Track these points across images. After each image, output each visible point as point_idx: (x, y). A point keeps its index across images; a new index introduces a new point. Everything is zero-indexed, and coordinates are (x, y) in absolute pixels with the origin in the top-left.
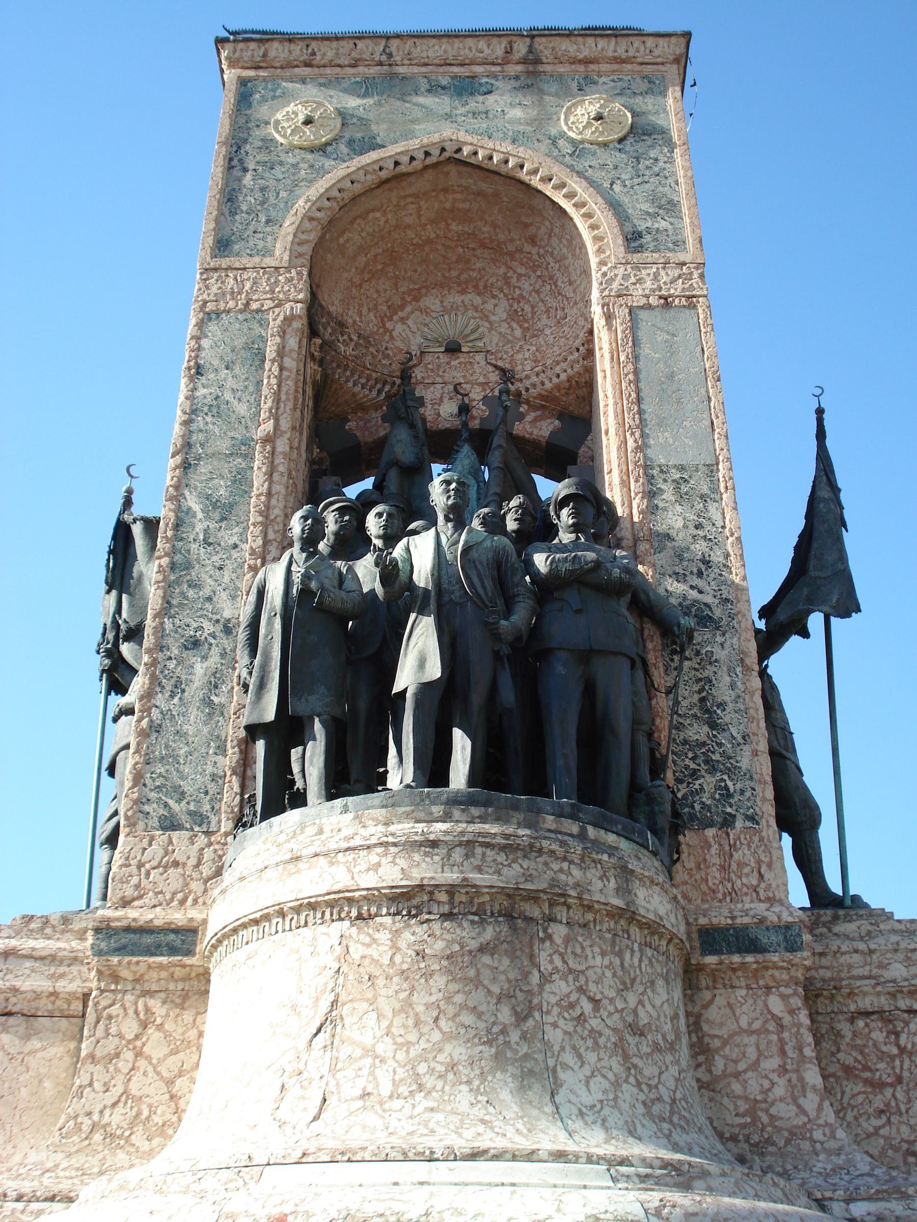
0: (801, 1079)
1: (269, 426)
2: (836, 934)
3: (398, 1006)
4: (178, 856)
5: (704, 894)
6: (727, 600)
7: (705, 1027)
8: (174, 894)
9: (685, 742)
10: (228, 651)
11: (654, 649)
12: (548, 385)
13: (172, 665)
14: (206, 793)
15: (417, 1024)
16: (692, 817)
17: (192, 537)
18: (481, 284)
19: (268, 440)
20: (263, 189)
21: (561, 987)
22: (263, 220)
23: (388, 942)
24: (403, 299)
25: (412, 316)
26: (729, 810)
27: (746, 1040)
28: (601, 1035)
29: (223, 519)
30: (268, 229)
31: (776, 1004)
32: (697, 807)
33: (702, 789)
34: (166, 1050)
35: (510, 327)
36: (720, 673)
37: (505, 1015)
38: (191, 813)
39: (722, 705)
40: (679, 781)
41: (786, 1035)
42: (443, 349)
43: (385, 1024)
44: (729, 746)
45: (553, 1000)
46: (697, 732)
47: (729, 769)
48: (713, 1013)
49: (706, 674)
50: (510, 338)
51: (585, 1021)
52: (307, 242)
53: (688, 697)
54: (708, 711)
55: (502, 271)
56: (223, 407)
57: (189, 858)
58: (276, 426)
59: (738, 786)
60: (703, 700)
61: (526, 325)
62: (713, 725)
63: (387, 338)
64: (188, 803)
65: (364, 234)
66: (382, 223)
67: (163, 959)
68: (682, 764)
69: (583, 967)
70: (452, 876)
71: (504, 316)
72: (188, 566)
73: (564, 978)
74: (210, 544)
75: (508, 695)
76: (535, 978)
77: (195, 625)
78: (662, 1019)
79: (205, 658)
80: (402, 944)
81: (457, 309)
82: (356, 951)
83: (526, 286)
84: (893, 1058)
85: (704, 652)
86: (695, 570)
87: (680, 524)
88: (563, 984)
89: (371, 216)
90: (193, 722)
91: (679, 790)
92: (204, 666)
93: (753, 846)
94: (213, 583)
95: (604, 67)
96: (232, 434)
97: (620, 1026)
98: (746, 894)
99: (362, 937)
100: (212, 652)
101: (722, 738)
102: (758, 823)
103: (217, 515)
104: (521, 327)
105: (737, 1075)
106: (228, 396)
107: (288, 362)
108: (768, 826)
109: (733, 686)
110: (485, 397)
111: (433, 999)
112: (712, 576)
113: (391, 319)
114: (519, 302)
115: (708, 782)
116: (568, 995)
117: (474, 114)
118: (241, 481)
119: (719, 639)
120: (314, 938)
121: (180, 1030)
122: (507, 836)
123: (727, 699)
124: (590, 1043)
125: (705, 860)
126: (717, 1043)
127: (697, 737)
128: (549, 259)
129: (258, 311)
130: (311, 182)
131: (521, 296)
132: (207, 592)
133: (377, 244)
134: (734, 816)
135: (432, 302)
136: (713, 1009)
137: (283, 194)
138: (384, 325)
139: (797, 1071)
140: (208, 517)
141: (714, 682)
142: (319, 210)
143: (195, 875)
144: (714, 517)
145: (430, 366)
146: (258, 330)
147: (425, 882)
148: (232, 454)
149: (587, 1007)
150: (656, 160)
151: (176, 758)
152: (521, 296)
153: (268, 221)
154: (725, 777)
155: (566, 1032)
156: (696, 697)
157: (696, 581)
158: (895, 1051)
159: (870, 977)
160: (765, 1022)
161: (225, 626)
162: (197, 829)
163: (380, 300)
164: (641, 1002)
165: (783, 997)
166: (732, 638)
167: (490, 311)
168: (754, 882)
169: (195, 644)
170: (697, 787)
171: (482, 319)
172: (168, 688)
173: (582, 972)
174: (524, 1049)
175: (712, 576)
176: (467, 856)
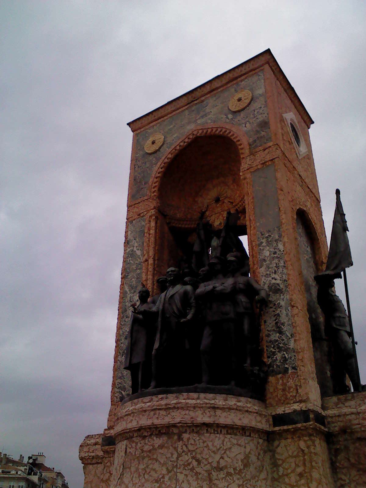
0: (311, 476)
1: (146, 256)
2: (346, 406)
9: (271, 341)
15: (140, 476)
16: (273, 371)
17: (127, 300)
19: (147, 260)
22: (143, 184)
23: (135, 447)
26: (286, 366)
28: (200, 474)
31: (302, 445)
32: (275, 367)
33: (277, 359)
36: (282, 311)
37: (164, 471)
39: (283, 324)
40: (269, 357)
41: (306, 457)
42: (214, 202)
44: (286, 340)
45: (182, 463)
46: (275, 336)
48: (279, 450)
49: (278, 312)
52: (156, 186)
58: (148, 255)
59: (289, 356)
60: (276, 323)
70: (149, 422)
71: (231, 182)
73: (186, 454)
76: (175, 456)
78: (235, 462)
80: (138, 447)
82: (128, 450)
85: (276, 304)
86: (274, 271)
87: (268, 254)
93: (294, 379)
95: (243, 78)
98: (292, 400)
101: (283, 337)
102: (297, 370)
103: (132, 291)
105: (287, 475)
106: (135, 249)
107: (152, 232)
108: (300, 370)
109: (287, 315)
115: (279, 356)
116: (187, 461)
122: (166, 405)
123: (285, 321)
124: (195, 478)
126: (280, 462)
127: (275, 338)
134: (288, 368)
136: (279, 448)
139: (310, 472)
140: (131, 293)
141: (280, 315)
142: (159, 173)
144: (280, 248)
147: (142, 425)
149: (195, 463)
150: (261, 107)
154: (285, 353)
155: (185, 475)
156: (275, 322)
159: (359, 424)
160: (298, 452)
164: (222, 458)
165: (305, 441)
166: (286, 295)
168: (294, 394)
170: (275, 358)
172: (121, 353)
173: (194, 451)
174: (168, 483)
176: (154, 414)
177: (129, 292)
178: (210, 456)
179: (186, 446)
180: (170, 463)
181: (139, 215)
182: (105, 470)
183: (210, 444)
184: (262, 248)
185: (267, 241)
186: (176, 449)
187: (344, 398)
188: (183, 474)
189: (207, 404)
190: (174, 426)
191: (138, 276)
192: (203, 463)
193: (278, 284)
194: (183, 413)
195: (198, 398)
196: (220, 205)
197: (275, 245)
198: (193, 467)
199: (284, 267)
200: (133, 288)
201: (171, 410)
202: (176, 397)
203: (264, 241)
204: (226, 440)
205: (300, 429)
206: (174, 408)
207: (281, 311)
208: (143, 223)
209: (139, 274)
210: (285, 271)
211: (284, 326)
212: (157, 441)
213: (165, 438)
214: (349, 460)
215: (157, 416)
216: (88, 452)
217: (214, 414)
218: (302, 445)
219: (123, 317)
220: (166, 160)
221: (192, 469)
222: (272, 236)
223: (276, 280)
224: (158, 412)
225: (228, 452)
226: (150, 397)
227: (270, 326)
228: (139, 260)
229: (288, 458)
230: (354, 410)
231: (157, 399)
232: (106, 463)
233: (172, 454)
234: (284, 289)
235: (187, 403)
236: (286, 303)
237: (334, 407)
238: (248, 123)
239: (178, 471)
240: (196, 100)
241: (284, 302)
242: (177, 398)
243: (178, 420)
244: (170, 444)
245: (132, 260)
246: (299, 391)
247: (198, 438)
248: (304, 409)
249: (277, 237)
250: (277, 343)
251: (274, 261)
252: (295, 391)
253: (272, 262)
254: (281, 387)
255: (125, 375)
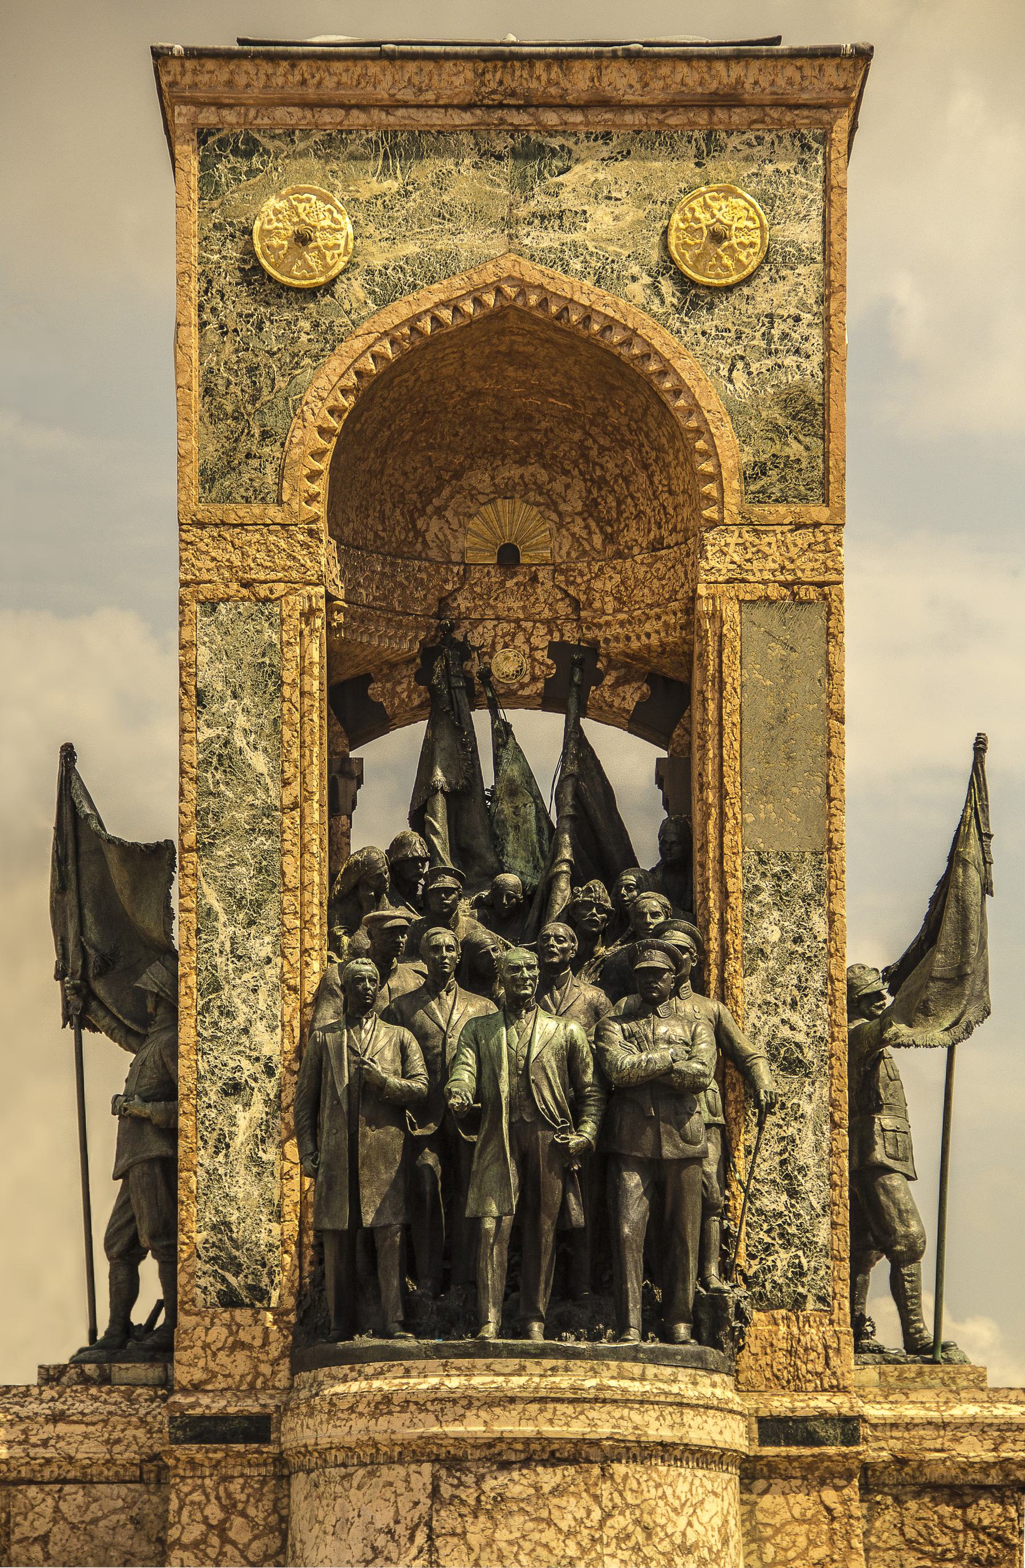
1: (296, 788)
3: (484, 1542)
4: (244, 1336)
5: (768, 1379)
6: (822, 1039)
7: (760, 1516)
8: (242, 1376)
9: (760, 1212)
10: (272, 1097)
11: (736, 1101)
12: (635, 645)
13: (213, 1113)
14: (264, 1265)
17: (217, 946)
18: (547, 452)
20: (252, 370)
21: (619, 1521)
22: (256, 431)
24: (439, 478)
25: (452, 504)
26: (800, 1290)
27: (797, 1529)
28: (652, 1559)
29: (251, 923)
30: (267, 450)
34: (250, 1536)
35: (587, 527)
37: (572, 1550)
38: (250, 1288)
39: (801, 1169)
40: (751, 1256)
43: (473, 1556)
45: (612, 1533)
46: (773, 1201)
47: (805, 1245)
49: (790, 1131)
50: (588, 547)
51: (640, 1549)
53: (767, 1164)
54: (788, 1177)
55: (577, 436)
56: (236, 758)
57: (254, 1338)
59: (812, 1264)
60: (783, 1163)
61: (609, 530)
62: (793, 1193)
63: (419, 547)
64: (246, 1277)
65: (387, 404)
66: (411, 383)
67: (240, 1447)
68: (756, 1238)
69: (638, 1502)
70: (528, 1429)
71: (579, 506)
72: (217, 988)
73: (622, 1513)
74: (239, 958)
75: (577, 1214)
76: (597, 1515)
77: (232, 1064)
78: (710, 1533)
79: (247, 1105)
81: (514, 488)
82: (446, 1491)
83: (610, 465)
84: (954, 1530)
87: (775, 936)
88: (621, 1518)
89: (397, 381)
90: (243, 1186)
91: (750, 1266)
92: (247, 1115)
94: (246, 1010)
96: (250, 799)
97: (669, 1548)
99: (450, 1480)
100: (254, 1098)
102: (829, 1305)
103: (241, 916)
104: (602, 530)
106: (239, 741)
109: (817, 1147)
110: (551, 644)
111: (512, 1537)
112: (807, 1007)
113: (423, 512)
114: (600, 489)
116: (625, 1529)
117: (543, 218)
118: (266, 869)
119: (808, 1089)
120: (408, 1475)
121: (261, 1515)
122: (574, 1389)
123: (810, 1162)
125: (772, 1345)
127: (774, 1206)
128: (642, 438)
129: (266, 600)
130: (316, 358)
131: (603, 478)
132: (240, 1021)
133: (404, 408)
135: (480, 480)
137: (281, 383)
138: (414, 526)
141: (798, 1142)
143: (263, 1357)
144: (816, 929)
145: (477, 589)
146: (269, 635)
147: (505, 1435)
148: (253, 830)
149: (640, 1536)
151: (228, 1225)
152: (603, 478)
153: (265, 435)
154: (800, 1253)
156: (777, 1159)
157: (787, 1014)
158: (958, 1525)
159: (942, 1450)
161: (266, 1065)
162: (258, 1305)
163: (408, 486)
164: (690, 1524)
167: (559, 495)
168: (820, 1369)
169: (234, 1089)
170: (770, 1263)
171: (548, 506)
173: (638, 1506)
175: (807, 1007)
176: (541, 1411)
177: (223, 917)
178: (669, 1520)
179: (621, 1495)
180: (585, 1532)
181: (246, 584)
182: (185, 1513)
183: (669, 1491)
184: (757, 909)
185: (777, 891)
186: (597, 1498)
187: (896, 1373)
188: (616, 1560)
189: (667, 1394)
190: (595, 1443)
191: (264, 863)
192: (657, 1534)
193: (798, 1045)
194: (617, 1414)
195: (643, 1378)
196: (516, 584)
197: (800, 912)
198: (637, 1543)
199: (823, 994)
200: (244, 907)
201: (587, 1406)
202: (592, 1369)
203: (766, 884)
204: (697, 1482)
205: (830, 1458)
206: (596, 1400)
207: (800, 1130)
208: (269, 635)
209: (266, 855)
210: (825, 1008)
211: (805, 1175)
212: (549, 1478)
213: (571, 1470)
214: (903, 1534)
215: (548, 1415)
216: (20, 1443)
217: (678, 1420)
218: (830, 1496)
219: (206, 1008)
220: (369, 365)
221: (637, 1549)
222: (795, 877)
223: (792, 1028)
224: (550, 1406)
225: (698, 1511)
226: (517, 1361)
227: (765, 1166)
228: (260, 793)
229: (788, 1523)
230: (934, 1415)
231: (538, 1370)
232: (187, 1495)
233: (589, 1512)
234: (815, 1068)
235: (624, 1391)
236: (817, 1111)
237: (879, 1399)
238: (740, 365)
239: (607, 1551)
240: (518, 107)
241: (813, 1105)
242: (596, 1373)
243: (605, 1430)
244: (582, 1487)
245: (227, 784)
246: (834, 1361)
247: (645, 1477)
248: (845, 1410)
249: (809, 887)
250: (780, 1222)
251: (793, 967)
252: (822, 1360)
253: (788, 968)
254: (784, 1345)
255: (234, 1219)
